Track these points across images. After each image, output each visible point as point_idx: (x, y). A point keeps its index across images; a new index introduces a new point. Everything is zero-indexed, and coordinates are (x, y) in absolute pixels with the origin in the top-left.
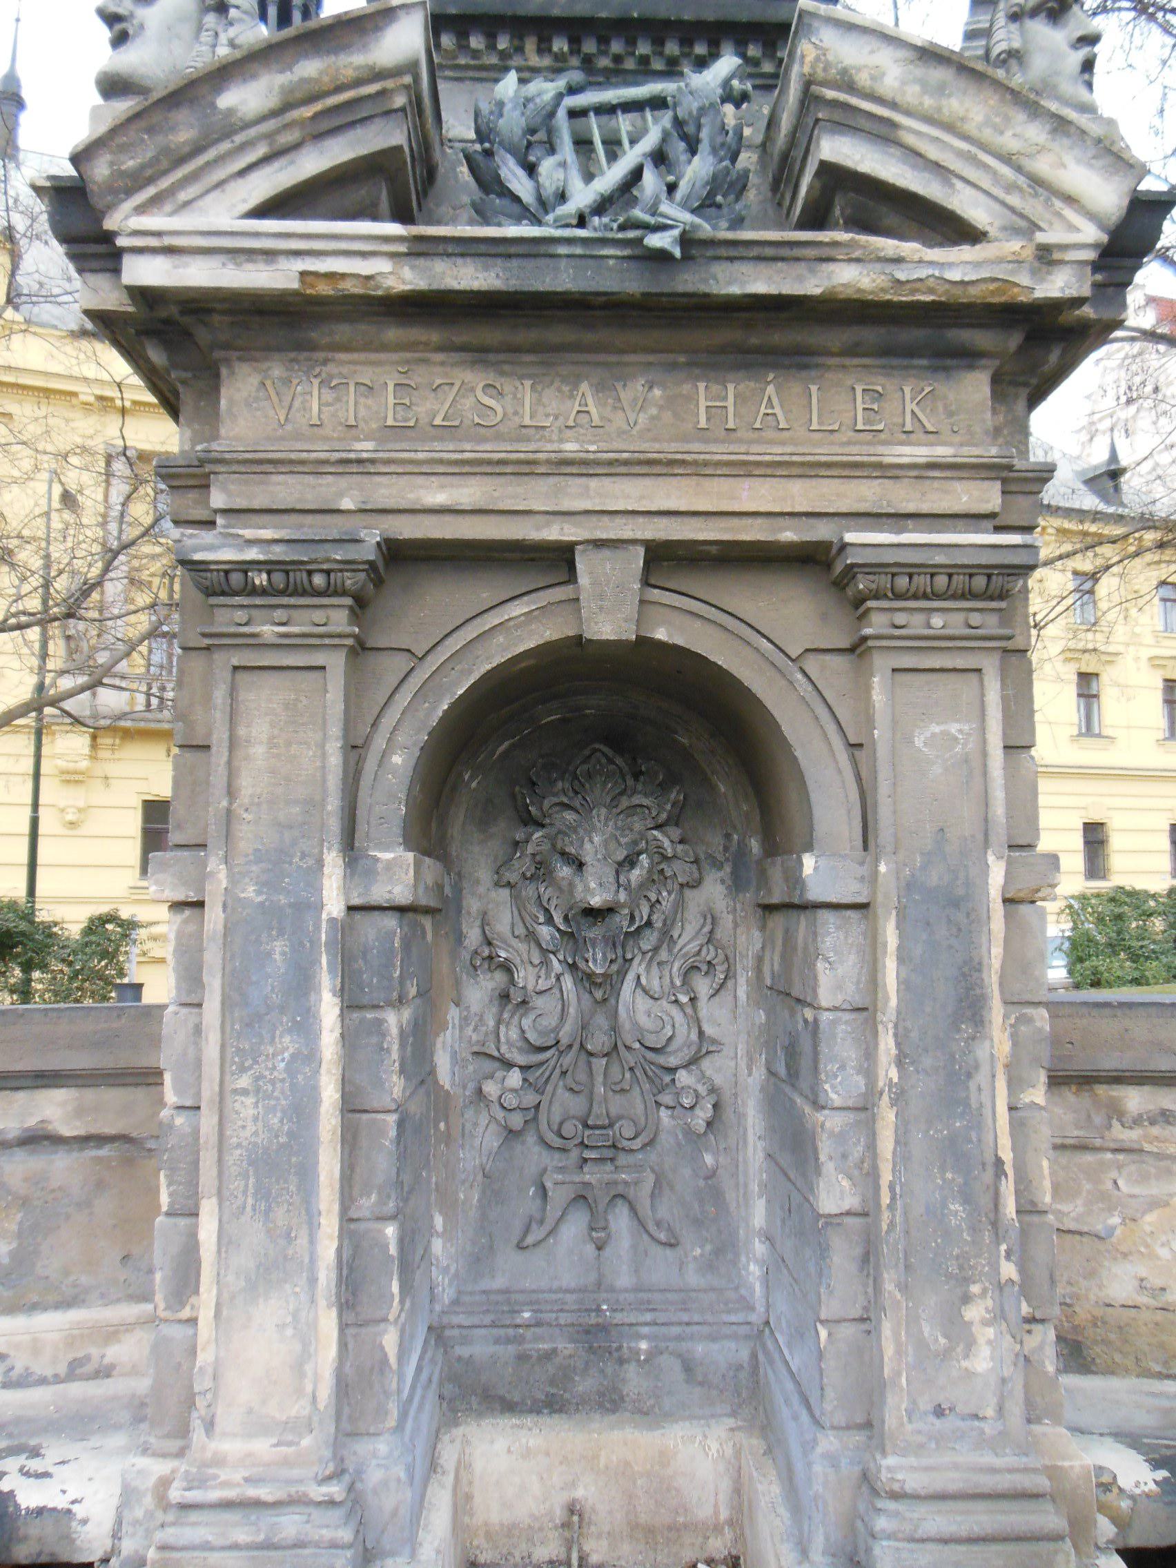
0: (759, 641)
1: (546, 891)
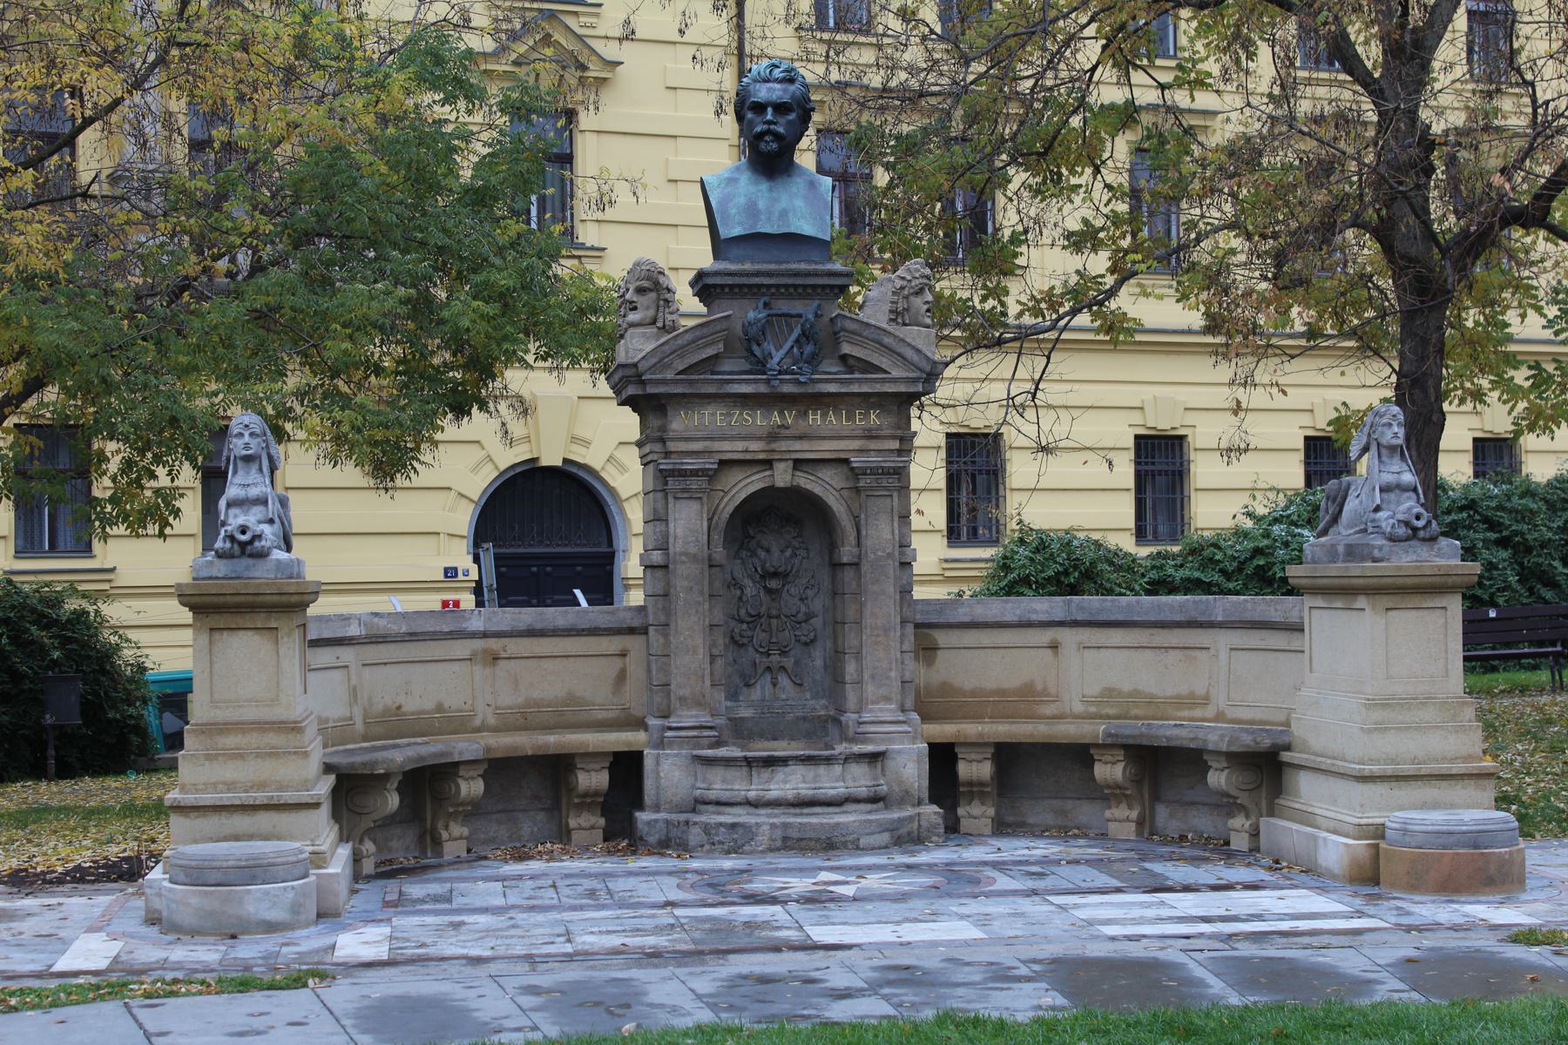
0: (827, 487)
1: (756, 561)
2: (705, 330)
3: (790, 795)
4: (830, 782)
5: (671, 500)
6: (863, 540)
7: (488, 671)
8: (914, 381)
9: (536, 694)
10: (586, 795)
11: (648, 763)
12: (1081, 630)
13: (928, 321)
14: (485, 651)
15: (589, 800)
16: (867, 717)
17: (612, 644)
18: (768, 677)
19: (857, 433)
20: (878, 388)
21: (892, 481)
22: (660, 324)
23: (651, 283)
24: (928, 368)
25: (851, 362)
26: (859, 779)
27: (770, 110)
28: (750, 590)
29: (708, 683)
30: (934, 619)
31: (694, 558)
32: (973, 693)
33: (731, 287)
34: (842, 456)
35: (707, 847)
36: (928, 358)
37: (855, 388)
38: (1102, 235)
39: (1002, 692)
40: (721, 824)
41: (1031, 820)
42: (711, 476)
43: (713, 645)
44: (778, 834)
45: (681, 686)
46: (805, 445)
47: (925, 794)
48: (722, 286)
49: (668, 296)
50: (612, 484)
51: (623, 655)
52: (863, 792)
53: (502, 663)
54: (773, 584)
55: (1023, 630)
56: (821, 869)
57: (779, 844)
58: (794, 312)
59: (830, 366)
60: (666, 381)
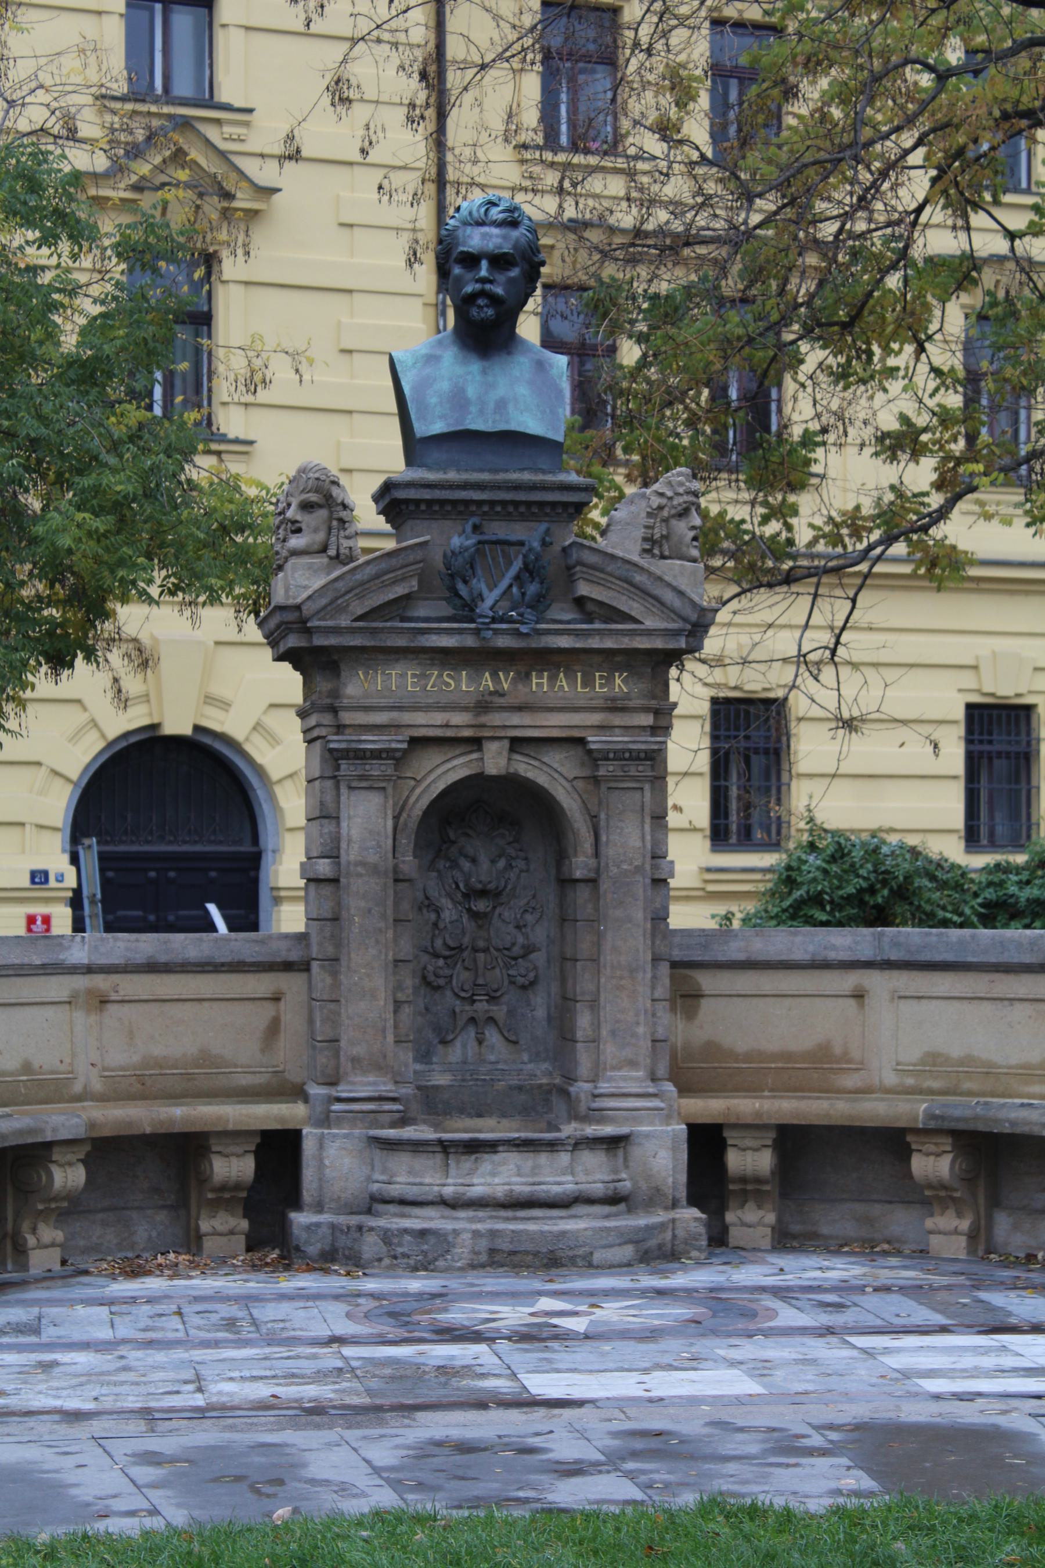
0: (555, 776)
2: (394, 562)
3: (499, 1191)
4: (555, 1175)
5: (344, 790)
6: (603, 850)
7: (93, 1018)
8: (675, 633)
9: (158, 1051)
10: (223, 1188)
11: (309, 1146)
12: (895, 973)
13: (695, 553)
14: (90, 992)
15: (227, 1195)
16: (604, 1087)
17: (261, 984)
18: (472, 1032)
19: (595, 703)
20: (626, 643)
21: (644, 769)
22: (332, 552)
23: (321, 497)
24: (694, 617)
25: (590, 607)
26: (593, 1172)
27: (484, 264)
29: (390, 1038)
30: (697, 956)
31: (375, 870)
32: (748, 1057)
33: (430, 503)
34: (576, 733)
35: (387, 1261)
36: (693, 604)
37: (595, 643)
38: (925, 437)
39: (787, 1056)
40: (406, 1231)
41: (825, 1230)
42: (398, 758)
43: (399, 987)
44: (483, 1244)
45: (354, 1044)
46: (526, 719)
47: (682, 1193)
48: (417, 502)
49: (344, 514)
50: (259, 759)
51: (276, 999)
52: (598, 1189)
53: (112, 1008)
55: (816, 973)
56: (541, 1293)
57: (484, 1258)
58: (513, 538)
59: (562, 613)
60: (339, 629)
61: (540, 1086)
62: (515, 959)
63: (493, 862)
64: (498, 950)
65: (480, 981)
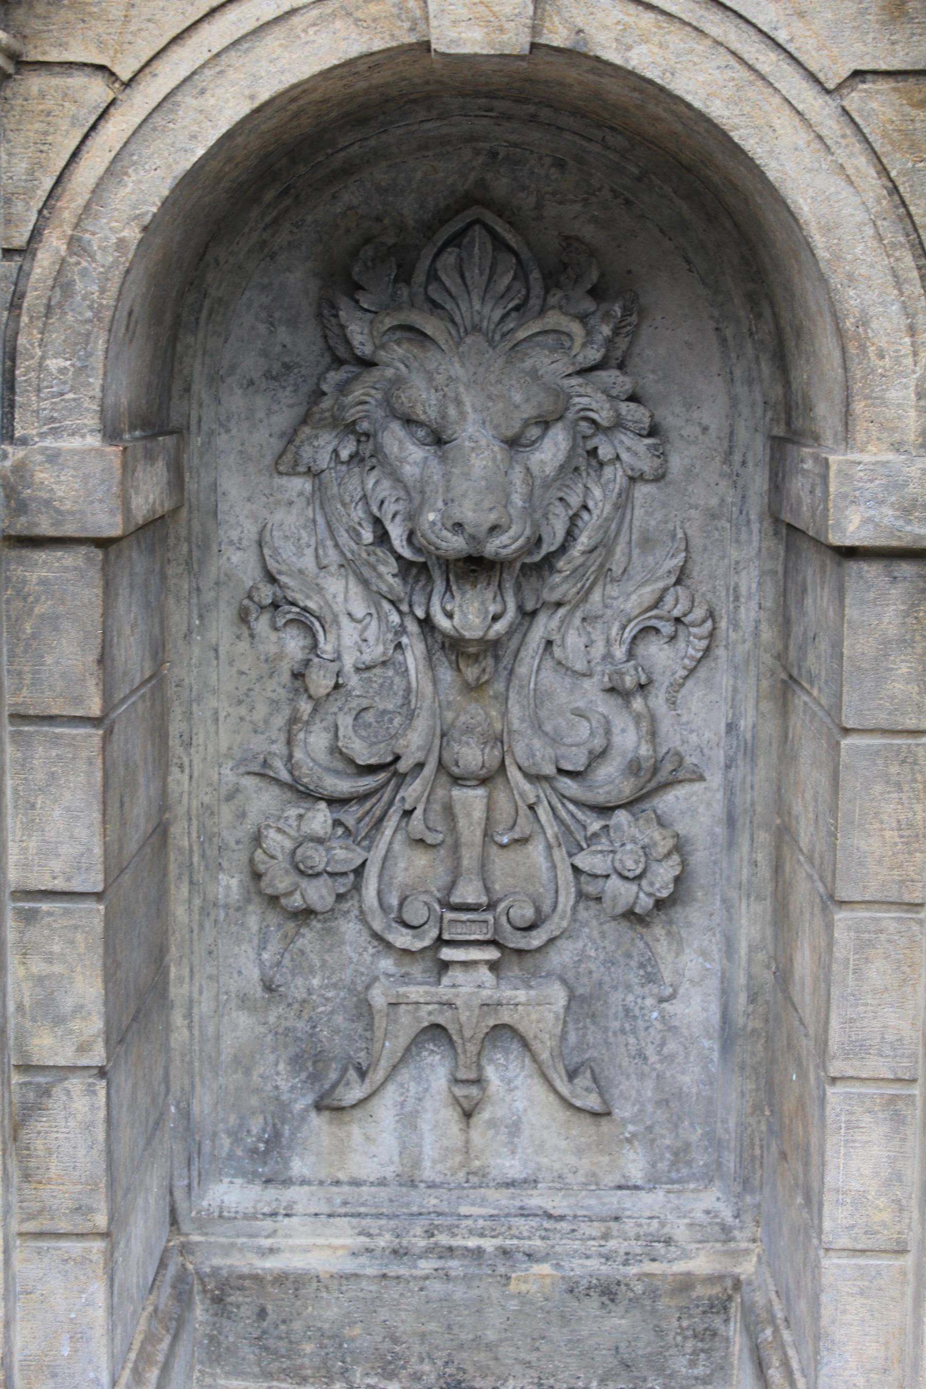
1: (378, 486)
28: (357, 627)
54: (469, 612)
61: (685, 1284)
62: (604, 810)
63: (514, 443)
64: (534, 778)
65: (469, 892)
